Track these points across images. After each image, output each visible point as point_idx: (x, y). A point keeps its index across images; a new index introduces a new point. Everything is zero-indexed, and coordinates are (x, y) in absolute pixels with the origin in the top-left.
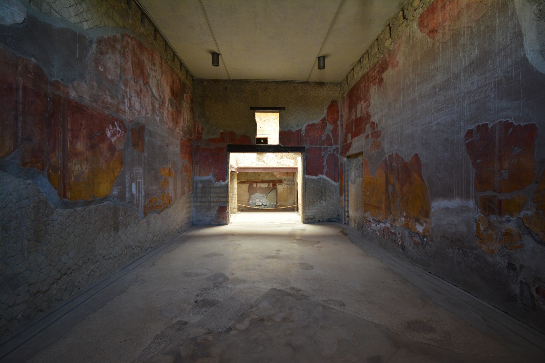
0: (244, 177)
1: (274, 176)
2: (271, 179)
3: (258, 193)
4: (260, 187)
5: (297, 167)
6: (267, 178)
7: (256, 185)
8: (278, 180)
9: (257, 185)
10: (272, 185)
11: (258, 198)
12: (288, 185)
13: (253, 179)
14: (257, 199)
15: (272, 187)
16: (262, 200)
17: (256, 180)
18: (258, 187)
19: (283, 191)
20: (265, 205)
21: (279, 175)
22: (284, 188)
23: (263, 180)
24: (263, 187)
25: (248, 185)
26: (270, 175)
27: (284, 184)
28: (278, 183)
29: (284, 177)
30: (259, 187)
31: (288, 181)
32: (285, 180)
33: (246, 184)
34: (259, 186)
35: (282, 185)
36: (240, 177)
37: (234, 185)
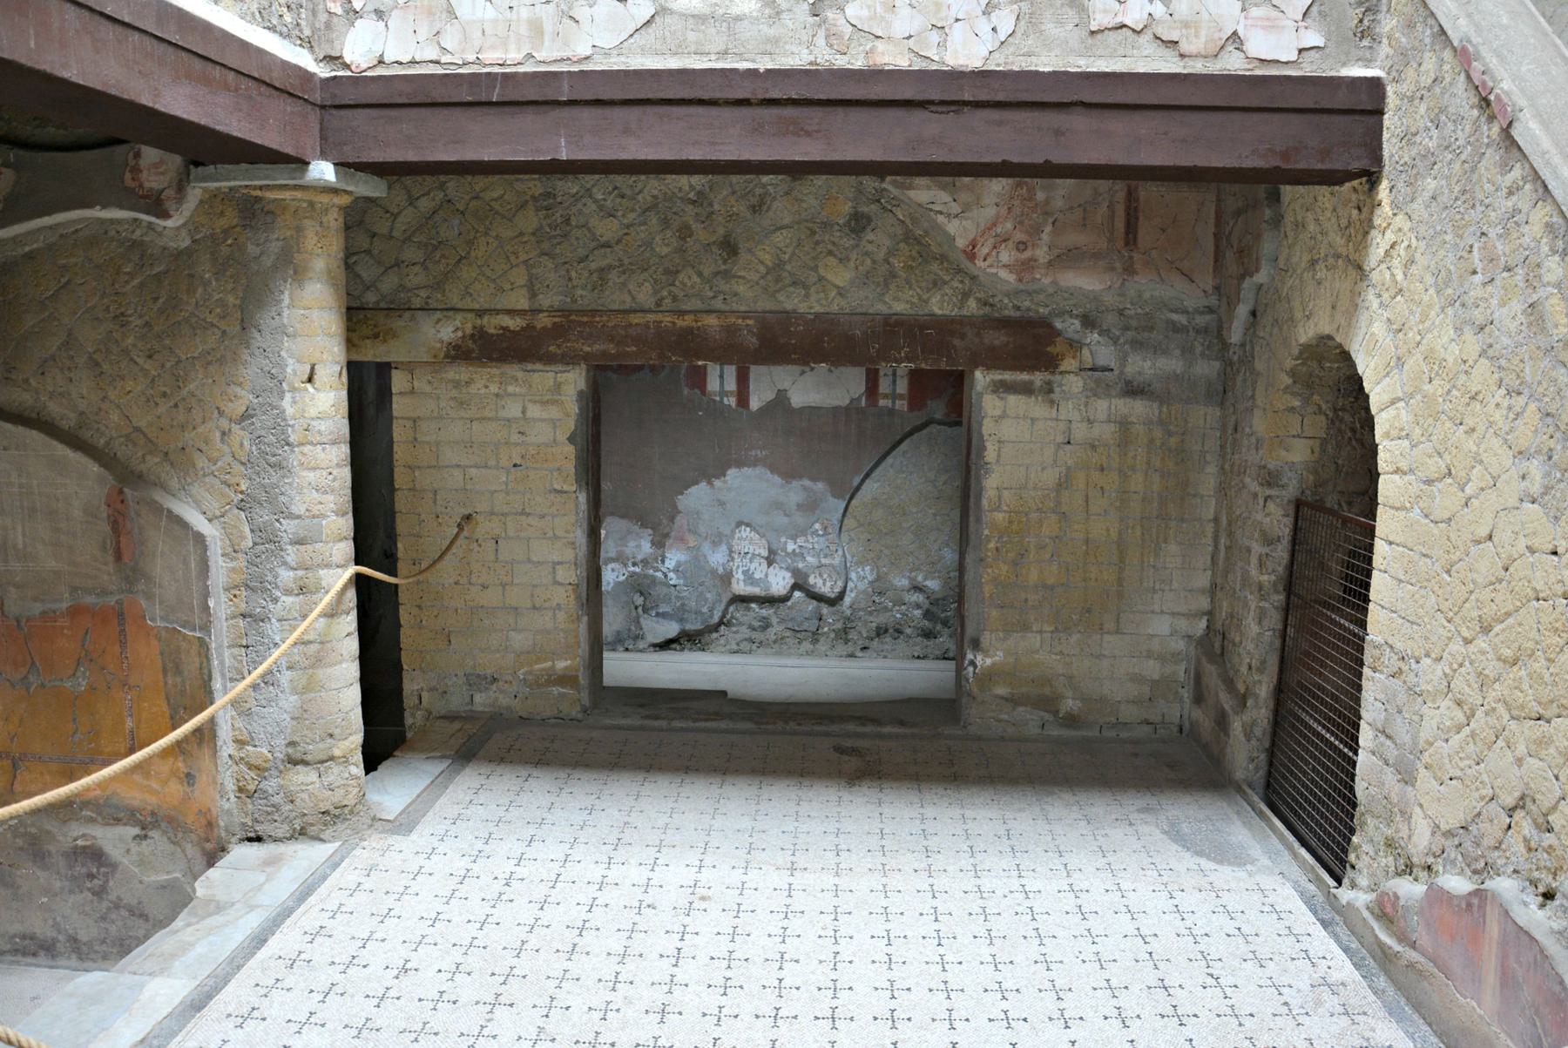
0: (519, 276)
1: (943, 258)
2: (899, 304)
3: (753, 463)
4: (781, 398)
5: (1376, 86)
6: (841, 292)
7: (731, 385)
8: (1005, 323)
9: (743, 379)
10: (902, 387)
11: (748, 525)
12: (1133, 390)
13: (645, 296)
14: (745, 532)
15: (902, 405)
16: (791, 547)
17: (688, 321)
18: (755, 404)
19: (1064, 484)
20: (819, 598)
21: (1006, 256)
22: (1080, 432)
23: (787, 316)
24: (812, 410)
25: (574, 380)
26: (878, 240)
27: (1075, 384)
28: (993, 360)
29: (1086, 282)
30: (768, 409)
31: (1137, 345)
32: (1088, 322)
33: (543, 377)
34: (770, 396)
35: (1048, 389)
36: (467, 273)
37: (277, 381)
